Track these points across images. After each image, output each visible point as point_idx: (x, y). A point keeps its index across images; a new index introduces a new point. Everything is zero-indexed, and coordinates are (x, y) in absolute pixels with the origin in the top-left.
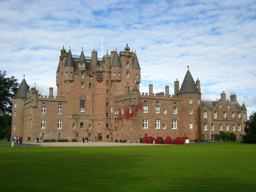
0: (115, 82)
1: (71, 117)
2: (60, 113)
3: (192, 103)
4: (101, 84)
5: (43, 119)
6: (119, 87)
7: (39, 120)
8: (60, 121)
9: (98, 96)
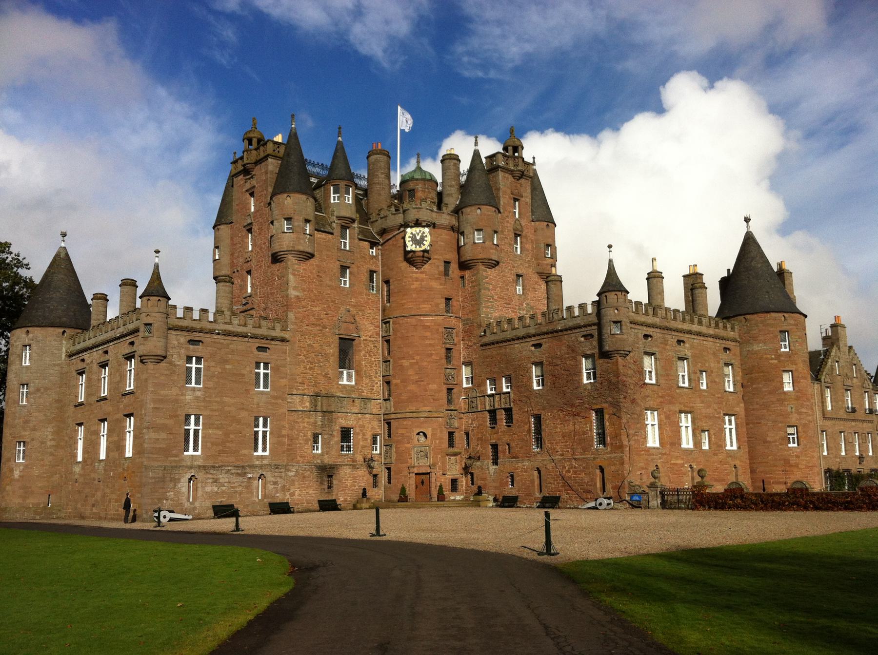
0: (482, 267)
1: (307, 404)
2: (264, 388)
3: (787, 350)
4: (421, 273)
5: (190, 411)
6: (494, 288)
7: (177, 416)
8: (261, 419)
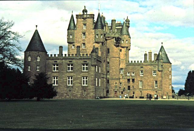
9: (114, 58)
